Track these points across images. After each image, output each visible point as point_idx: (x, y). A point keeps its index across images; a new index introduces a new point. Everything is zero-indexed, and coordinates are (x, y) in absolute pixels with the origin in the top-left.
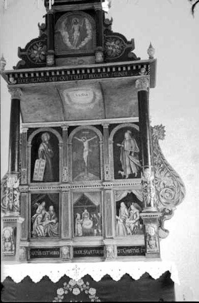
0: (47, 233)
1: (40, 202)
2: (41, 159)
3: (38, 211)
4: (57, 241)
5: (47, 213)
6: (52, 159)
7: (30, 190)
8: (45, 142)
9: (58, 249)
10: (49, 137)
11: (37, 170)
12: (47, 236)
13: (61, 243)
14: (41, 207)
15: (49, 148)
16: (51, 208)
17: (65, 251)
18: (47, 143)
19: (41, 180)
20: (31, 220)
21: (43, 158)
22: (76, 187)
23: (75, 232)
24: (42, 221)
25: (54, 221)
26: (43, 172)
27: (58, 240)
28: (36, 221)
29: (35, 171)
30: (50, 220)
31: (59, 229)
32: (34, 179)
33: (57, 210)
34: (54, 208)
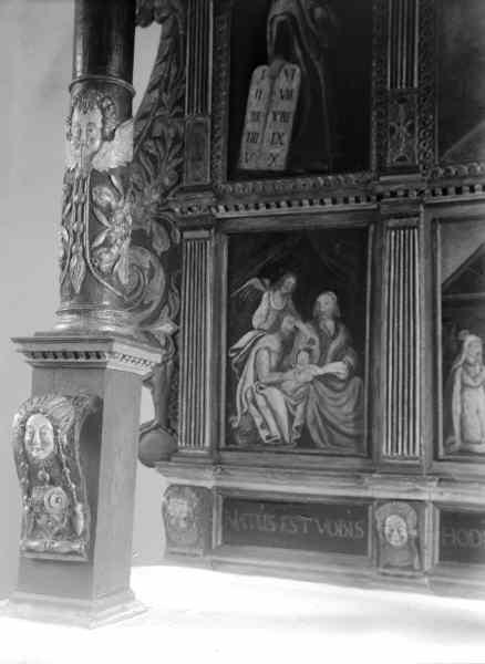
0: (304, 430)
1: (273, 275)
3: (258, 319)
4: (356, 476)
5: (302, 327)
7: (222, 213)
9: (358, 511)
11: (256, 116)
12: (304, 441)
13: (377, 489)
14: (271, 302)
16: (326, 302)
17: (395, 528)
19: (280, 165)
20: (229, 359)
21: (289, 57)
22: (459, 191)
23: (448, 429)
24: (280, 367)
25: (338, 368)
26: (285, 130)
27: (356, 463)
28: (251, 363)
29: (249, 126)
30: (321, 364)
31: (366, 414)
32: (246, 165)
33: (357, 322)
34: (342, 303)
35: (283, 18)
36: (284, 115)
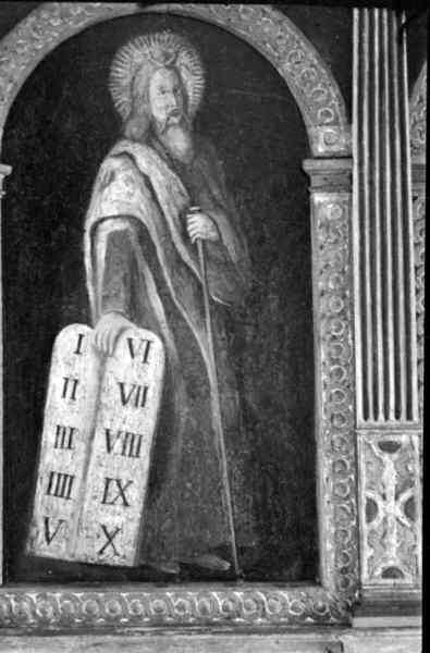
2: (109, 322)
6: (228, 322)
8: (151, 136)
10: (194, 83)
11: (66, 437)
15: (194, 201)
18: (179, 142)
19: (124, 552)
21: (136, 312)
26: (136, 472)
29: (52, 458)
35: (120, 226)
36: (131, 443)
